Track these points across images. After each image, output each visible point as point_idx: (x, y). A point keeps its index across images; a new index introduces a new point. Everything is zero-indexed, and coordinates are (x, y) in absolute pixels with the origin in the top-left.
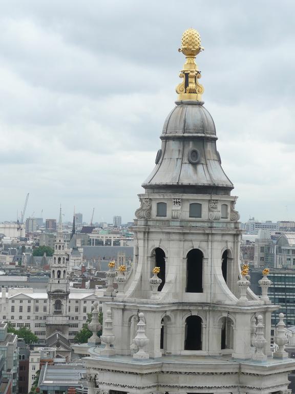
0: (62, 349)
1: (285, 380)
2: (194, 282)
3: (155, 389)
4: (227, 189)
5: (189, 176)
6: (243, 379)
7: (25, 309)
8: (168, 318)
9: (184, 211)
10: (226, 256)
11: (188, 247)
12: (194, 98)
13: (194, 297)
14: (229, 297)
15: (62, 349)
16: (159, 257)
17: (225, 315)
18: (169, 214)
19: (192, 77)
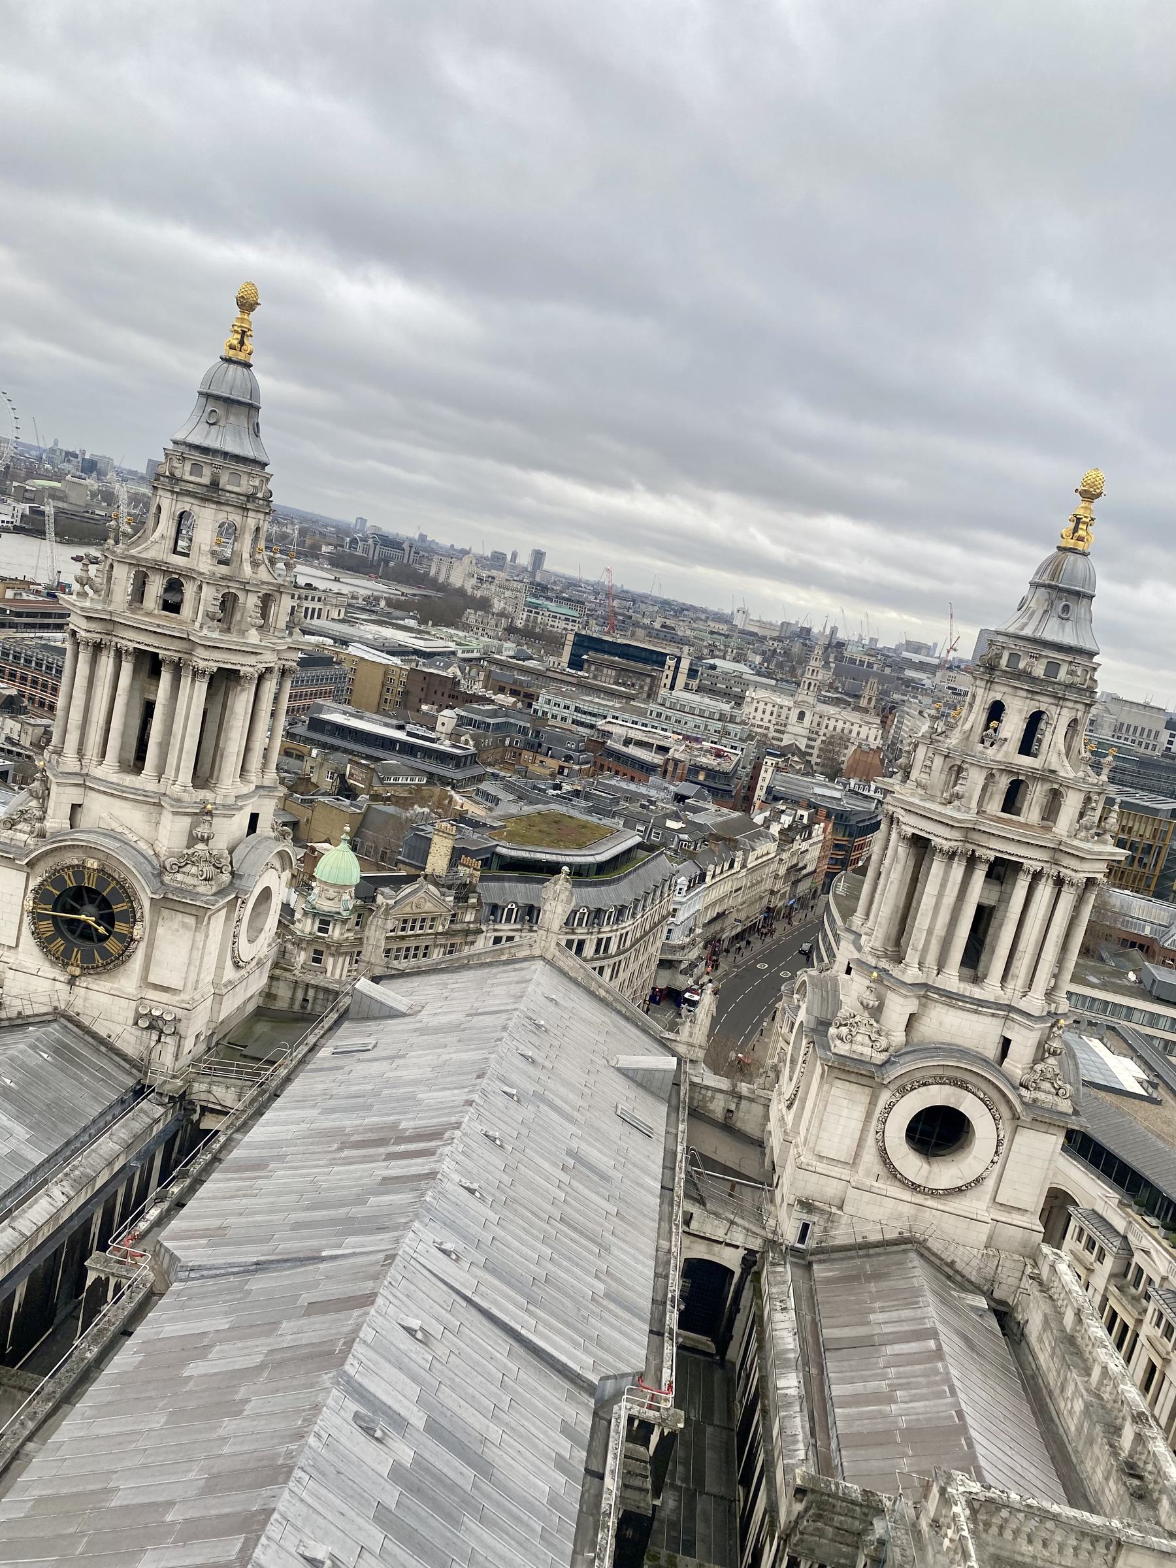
0: (796, 759)
1: (1103, 867)
2: (1027, 746)
3: (961, 844)
4: (1091, 654)
5: (1054, 632)
6: (1058, 856)
7: (768, 712)
8: (992, 775)
9: (1039, 670)
10: (1073, 724)
11: (1032, 707)
12: (1081, 546)
13: (1026, 761)
14: (1066, 771)
15: (796, 759)
16: (996, 711)
17: (1056, 786)
18: (1021, 665)
19: (1084, 523)
